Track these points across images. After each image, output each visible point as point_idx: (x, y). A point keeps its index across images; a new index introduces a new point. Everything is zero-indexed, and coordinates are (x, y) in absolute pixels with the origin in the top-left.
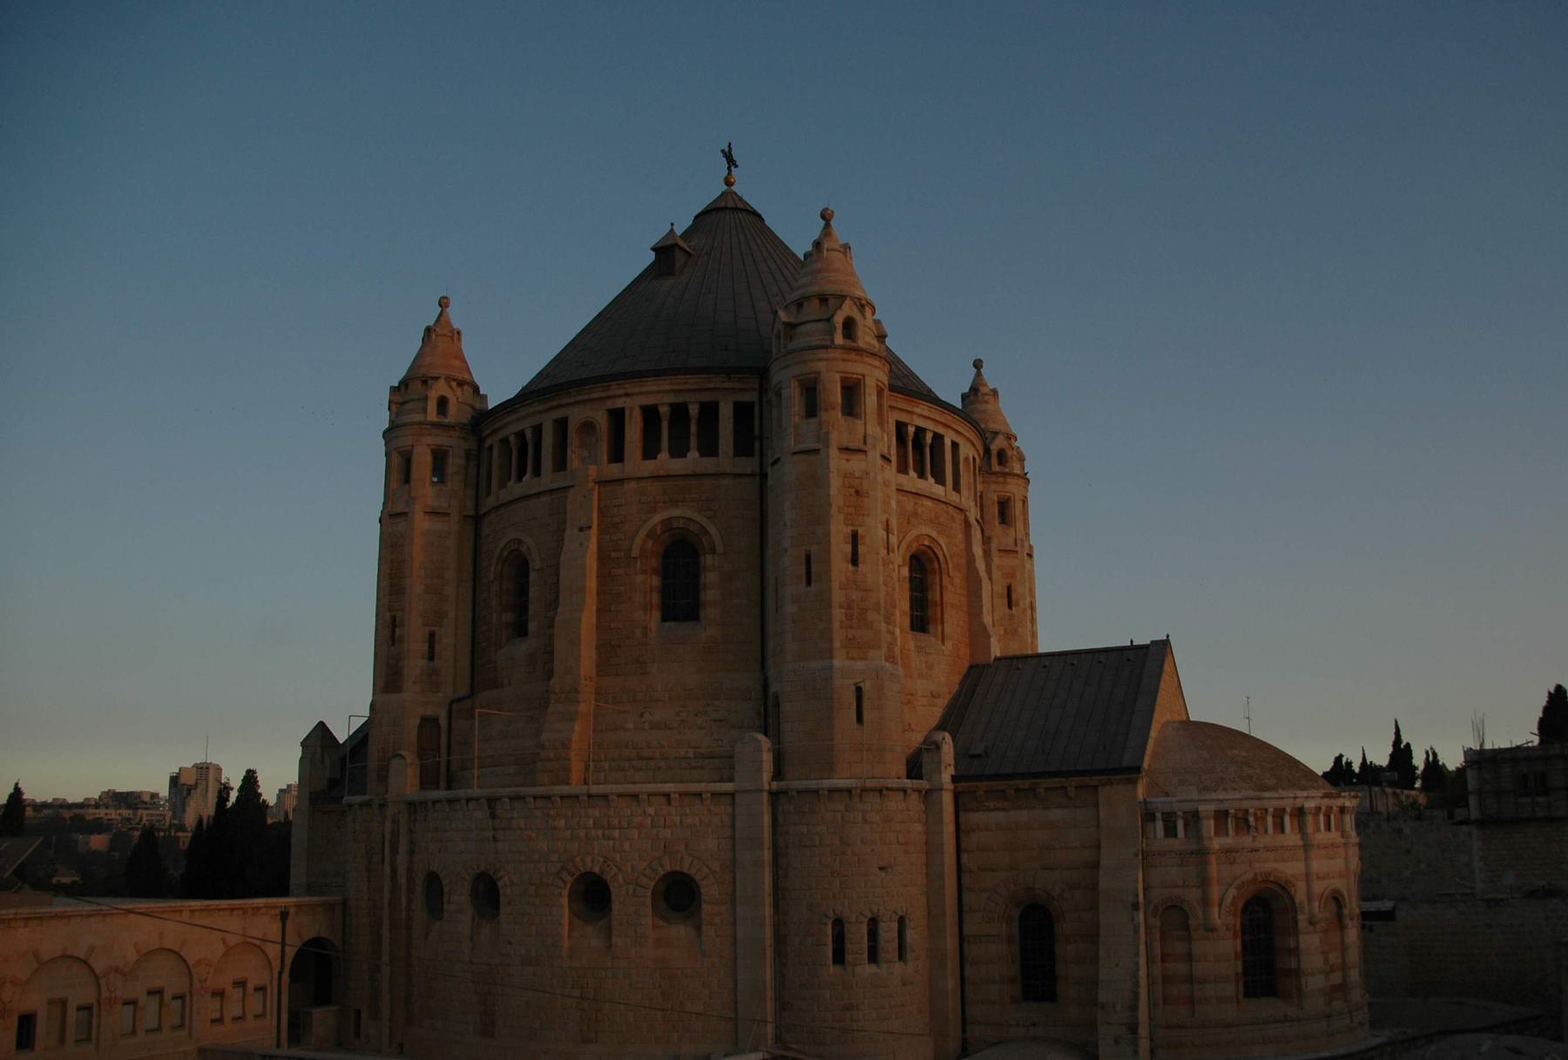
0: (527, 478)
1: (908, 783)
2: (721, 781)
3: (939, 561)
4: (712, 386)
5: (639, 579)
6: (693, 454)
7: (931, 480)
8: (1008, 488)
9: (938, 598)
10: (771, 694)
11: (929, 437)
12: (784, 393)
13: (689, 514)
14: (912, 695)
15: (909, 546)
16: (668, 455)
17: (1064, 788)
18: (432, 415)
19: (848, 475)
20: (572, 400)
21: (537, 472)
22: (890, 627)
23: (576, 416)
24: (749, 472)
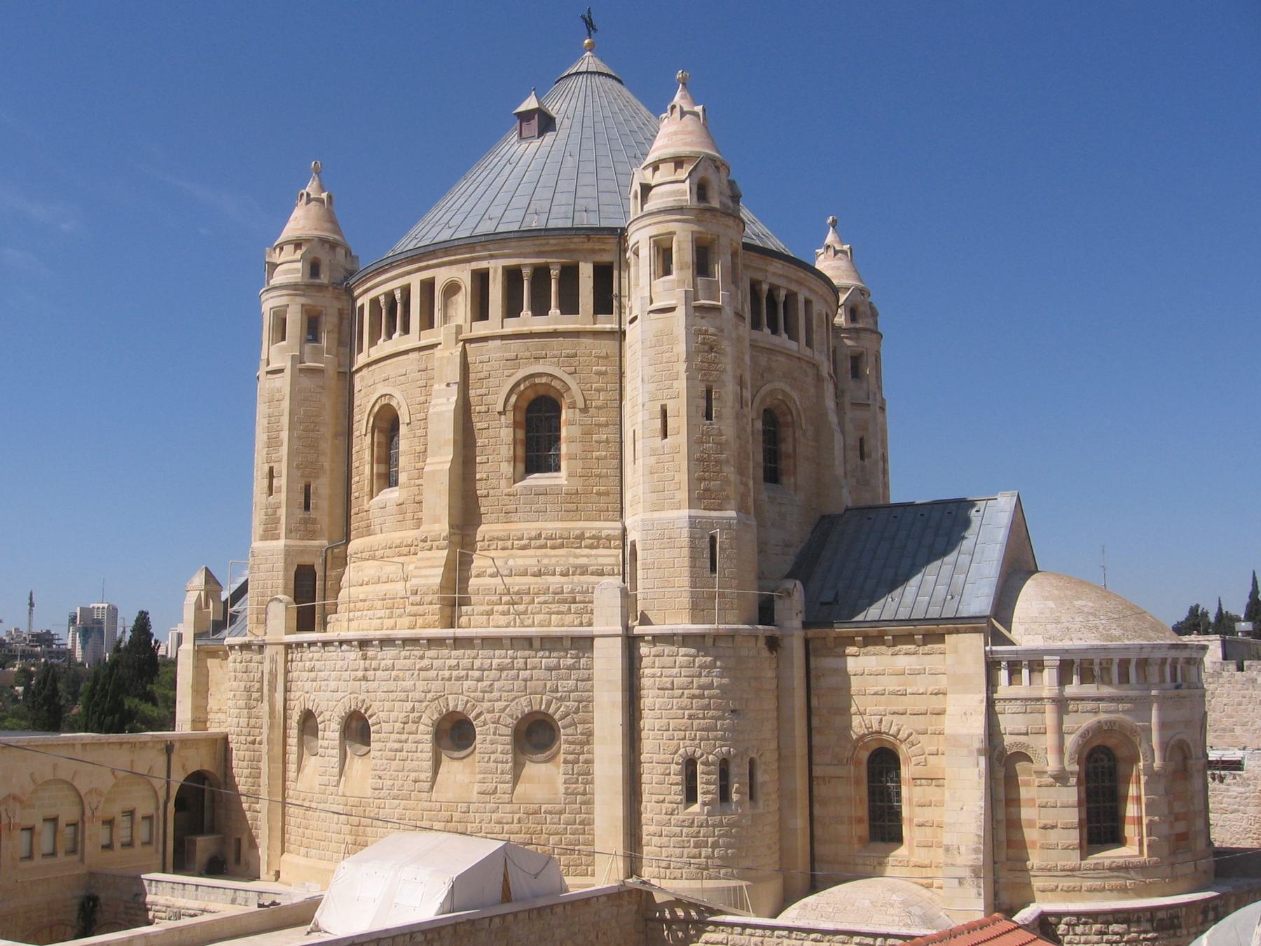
0: (396, 336)
2: (581, 625)
3: (792, 413)
4: (572, 246)
6: (554, 311)
7: (785, 336)
9: (790, 450)
11: (783, 293)
15: (763, 400)
16: (530, 313)
20: (440, 260)
21: (406, 330)
22: (744, 479)
23: (442, 276)
24: (608, 327)
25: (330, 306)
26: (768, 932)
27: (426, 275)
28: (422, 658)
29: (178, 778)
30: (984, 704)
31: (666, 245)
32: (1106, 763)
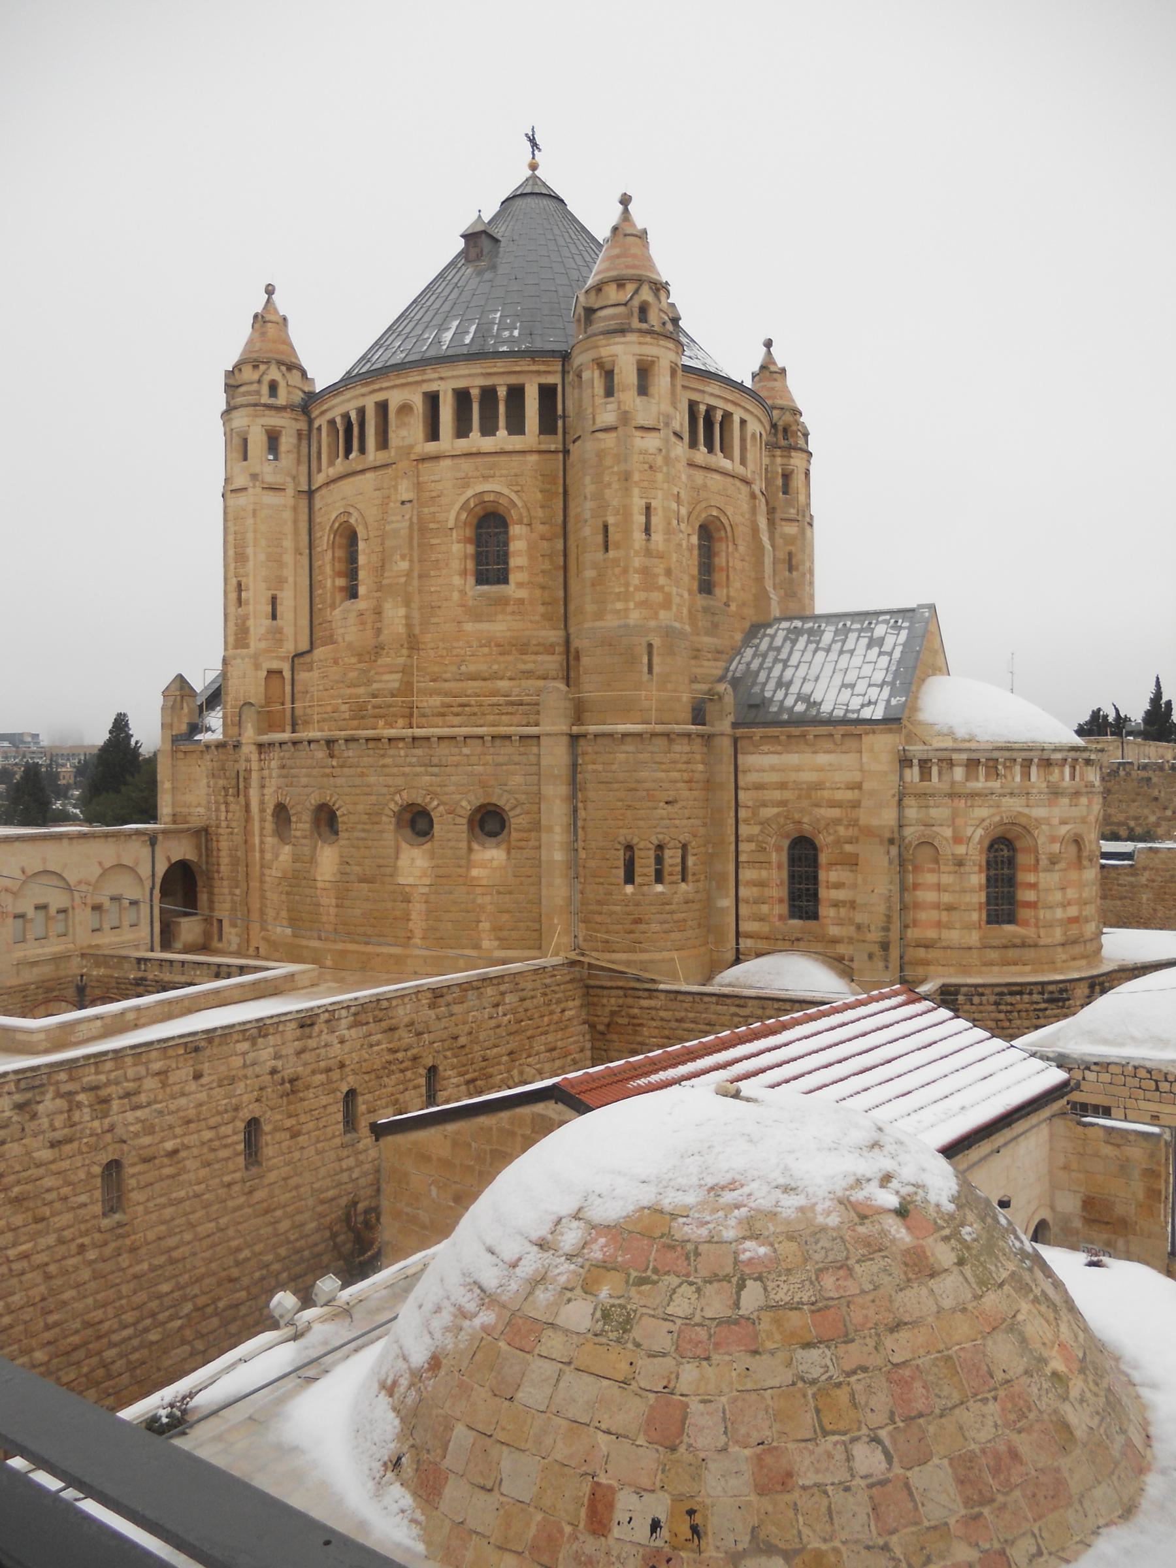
1: (693, 728)
4: (518, 369)
5: (457, 548)
6: (502, 433)
7: (721, 455)
8: (792, 461)
9: (724, 564)
10: (572, 650)
11: (719, 416)
12: (586, 375)
13: (497, 488)
14: (698, 650)
15: (698, 515)
17: (832, 735)
18: (265, 399)
19: (644, 452)
21: (362, 450)
24: (553, 447)
25: (289, 426)
26: (697, 998)
27: (380, 397)
28: (383, 756)
29: (161, 869)
30: (897, 798)
31: (608, 367)
32: (1006, 853)
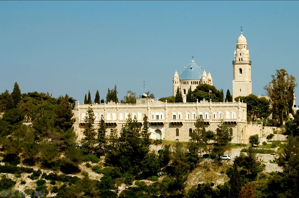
21: (186, 84)
